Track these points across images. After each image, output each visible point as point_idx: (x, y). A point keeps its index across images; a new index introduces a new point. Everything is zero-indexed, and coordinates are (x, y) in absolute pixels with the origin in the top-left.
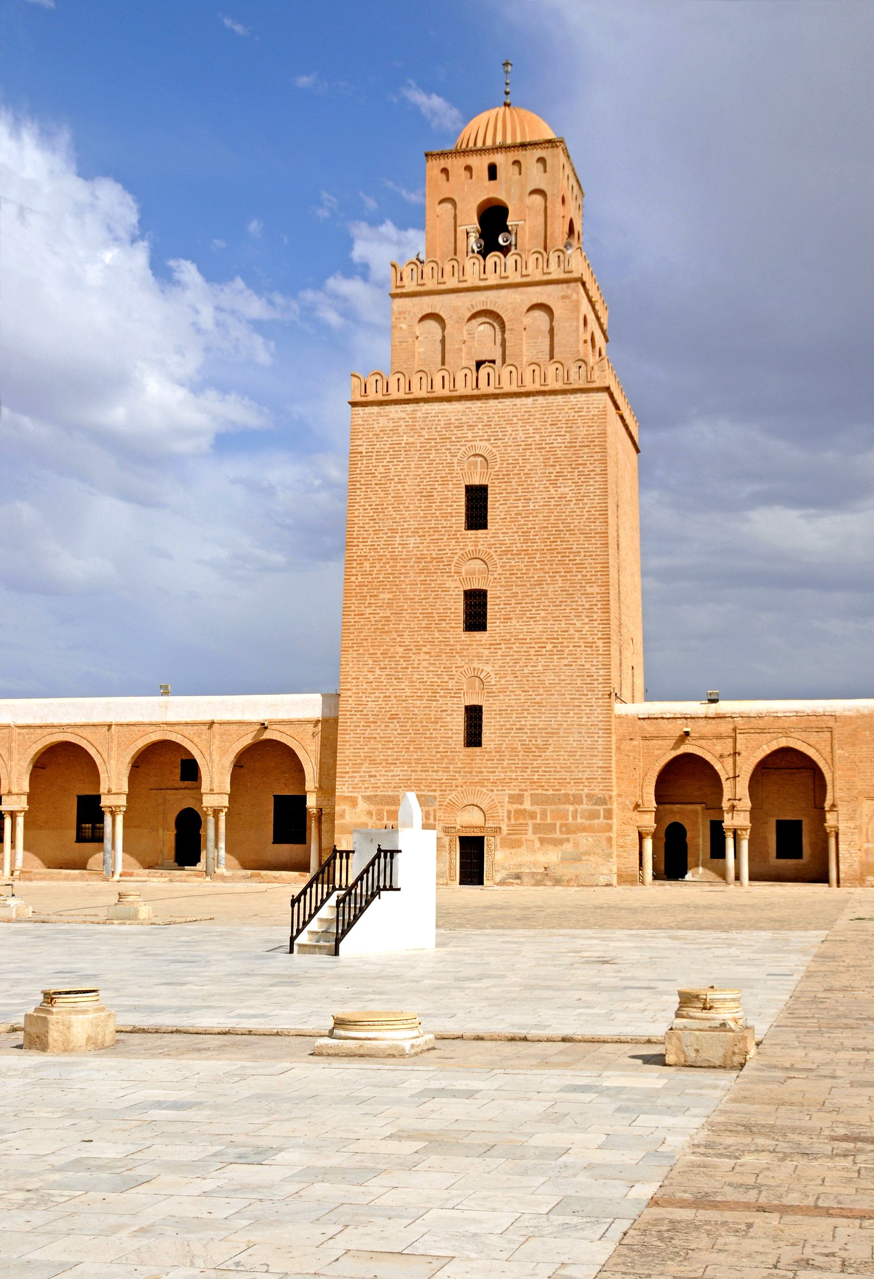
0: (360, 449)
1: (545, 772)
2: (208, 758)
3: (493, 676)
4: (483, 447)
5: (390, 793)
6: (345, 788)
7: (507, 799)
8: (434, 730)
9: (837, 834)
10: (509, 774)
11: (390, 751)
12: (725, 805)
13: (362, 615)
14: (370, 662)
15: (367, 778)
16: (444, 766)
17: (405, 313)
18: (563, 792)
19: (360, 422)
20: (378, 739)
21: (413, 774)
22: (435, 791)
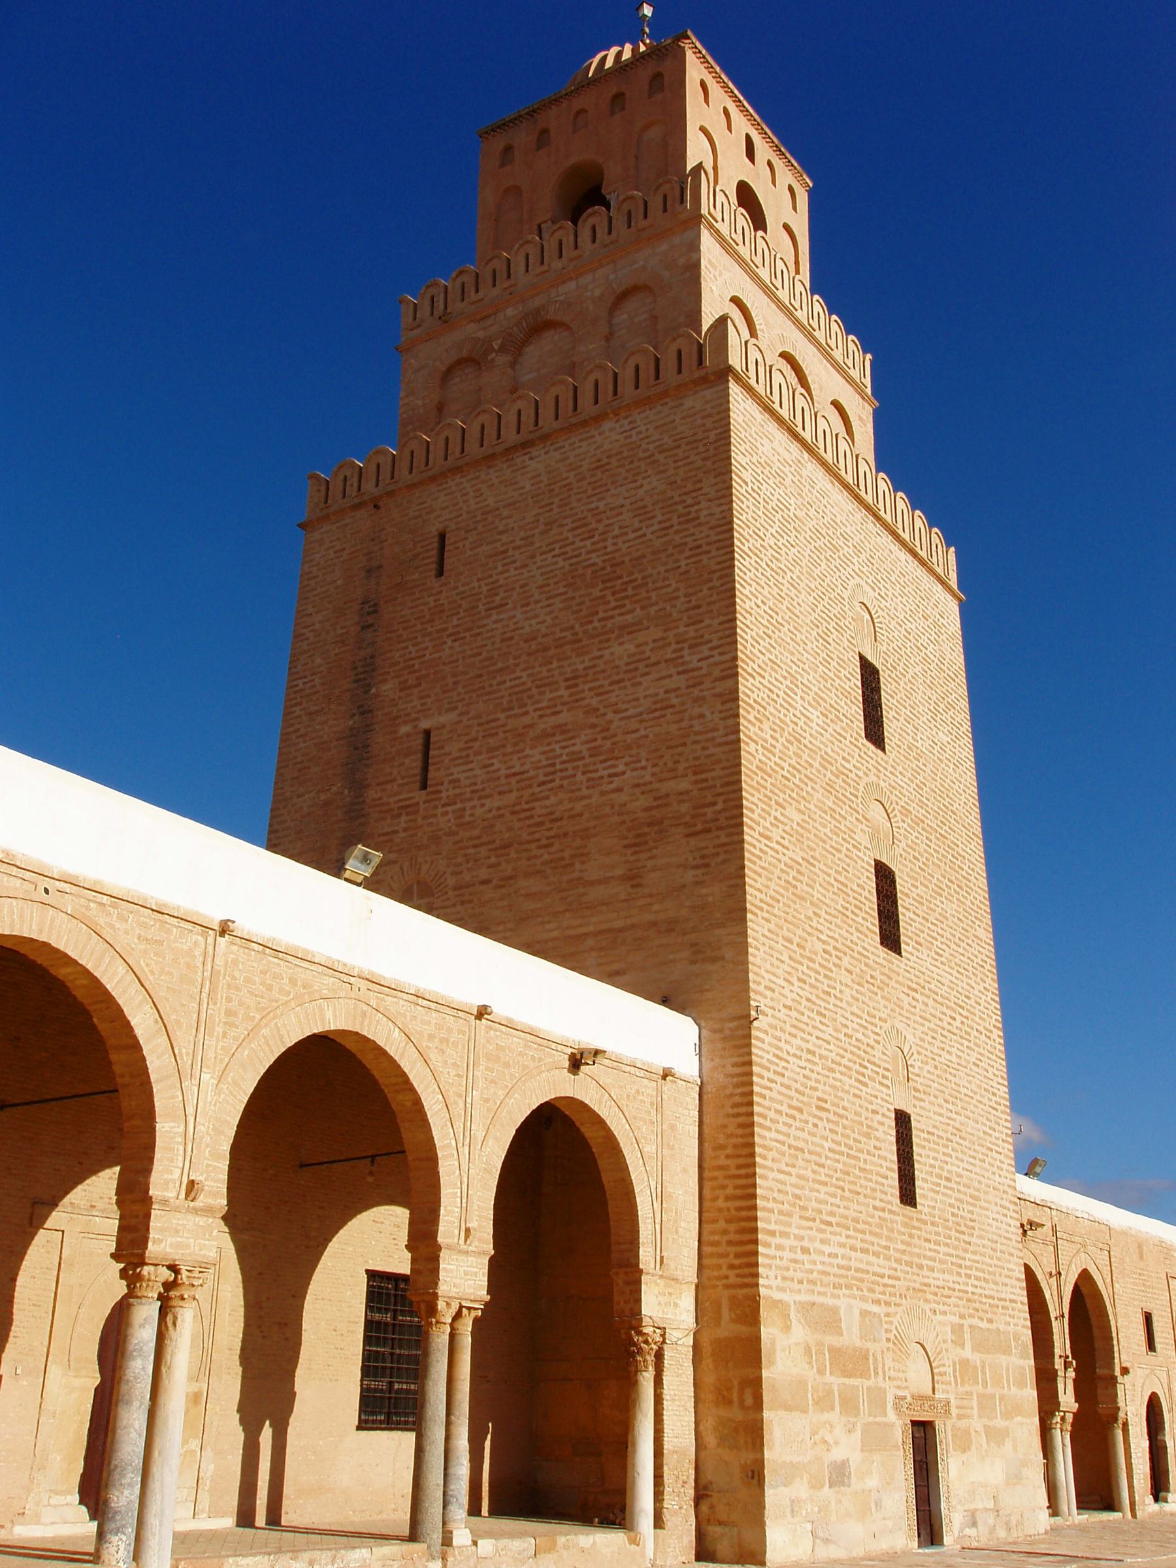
0: (746, 475)
1: (977, 1278)
2: (459, 1125)
3: (916, 1056)
4: (869, 596)
5: (830, 1301)
6: (772, 1274)
7: (949, 1336)
8: (869, 1153)
9: (1125, 1425)
10: (946, 1277)
11: (823, 1189)
12: (1058, 1364)
13: (768, 838)
14: (785, 958)
15: (799, 1256)
16: (884, 1243)
17: (715, 268)
18: (994, 1326)
19: (740, 421)
20: (807, 1155)
21: (853, 1254)
22: (877, 1302)
